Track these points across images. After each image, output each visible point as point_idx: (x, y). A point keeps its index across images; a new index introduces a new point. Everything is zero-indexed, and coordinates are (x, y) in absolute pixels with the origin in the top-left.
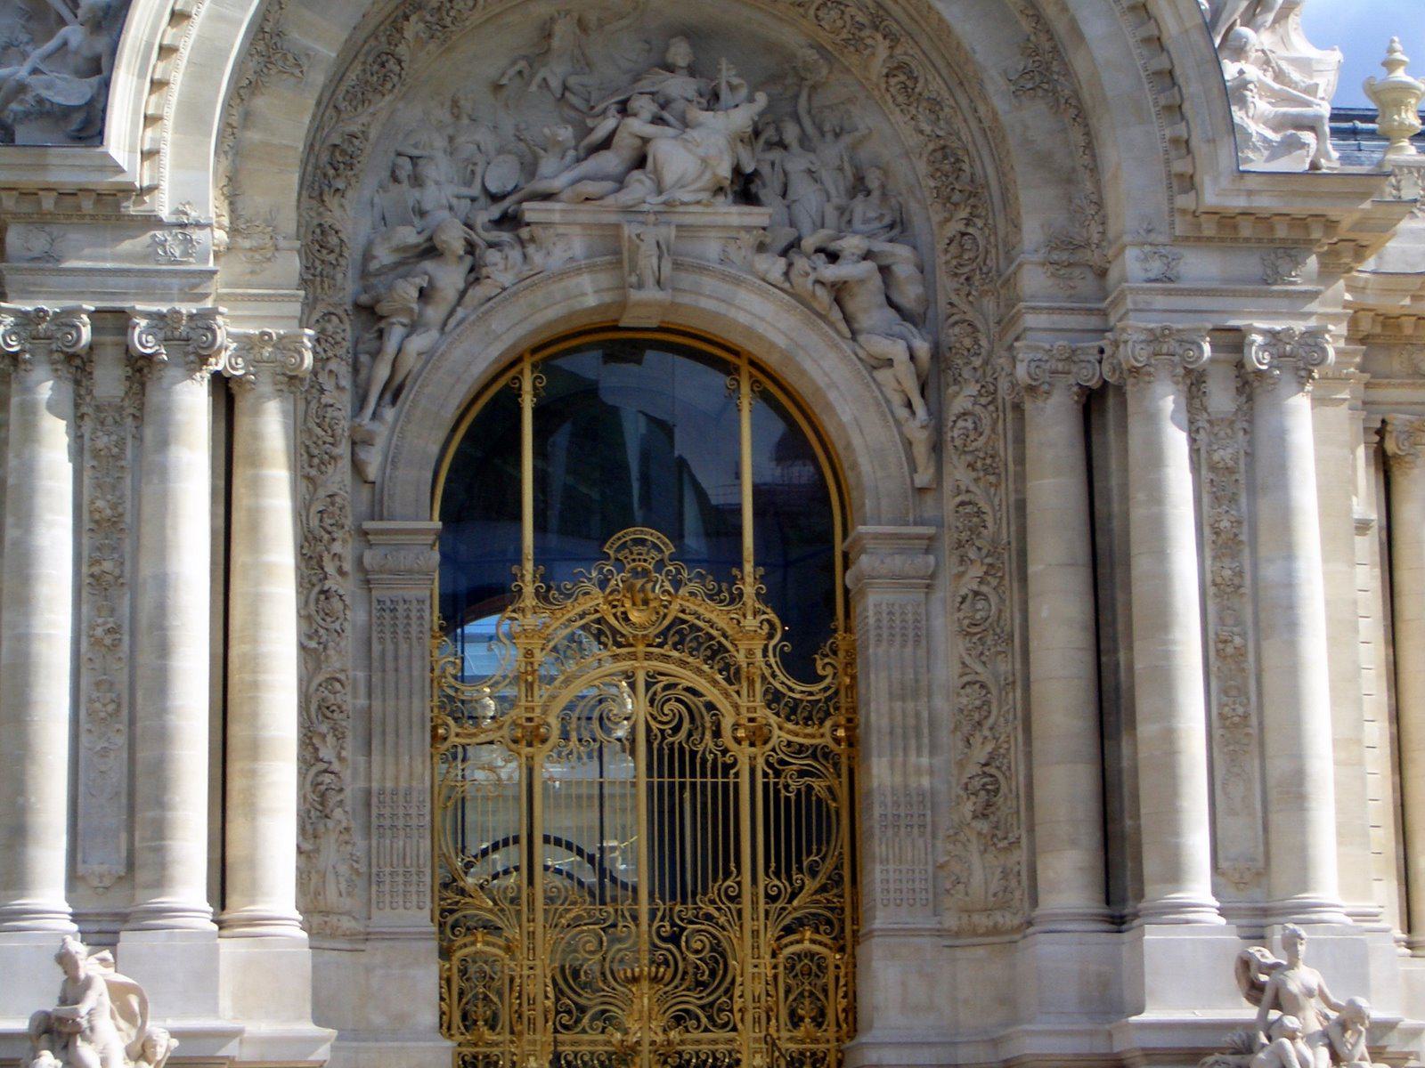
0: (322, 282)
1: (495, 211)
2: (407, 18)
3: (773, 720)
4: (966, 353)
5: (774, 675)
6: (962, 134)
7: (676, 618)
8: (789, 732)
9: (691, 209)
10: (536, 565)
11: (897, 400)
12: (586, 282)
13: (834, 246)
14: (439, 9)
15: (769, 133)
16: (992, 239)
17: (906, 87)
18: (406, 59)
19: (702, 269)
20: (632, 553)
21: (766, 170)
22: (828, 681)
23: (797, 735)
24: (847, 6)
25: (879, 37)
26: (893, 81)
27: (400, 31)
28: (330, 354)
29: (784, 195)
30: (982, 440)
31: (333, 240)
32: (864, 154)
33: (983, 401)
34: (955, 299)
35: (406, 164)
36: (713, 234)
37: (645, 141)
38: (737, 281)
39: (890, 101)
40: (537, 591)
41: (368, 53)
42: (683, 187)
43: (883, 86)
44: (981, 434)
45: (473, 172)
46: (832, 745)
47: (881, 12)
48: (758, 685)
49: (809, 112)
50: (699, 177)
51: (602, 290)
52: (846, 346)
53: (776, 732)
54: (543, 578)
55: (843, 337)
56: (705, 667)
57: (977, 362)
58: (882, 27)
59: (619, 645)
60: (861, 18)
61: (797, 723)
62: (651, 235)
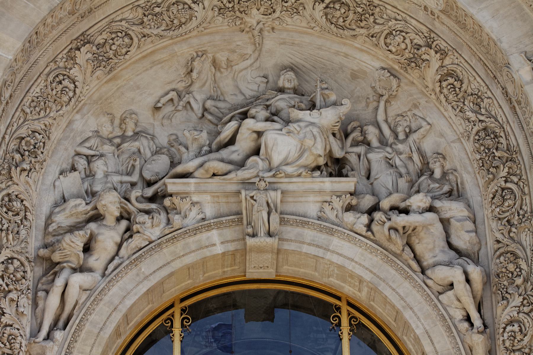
0: (7, 234)
1: (150, 192)
2: (78, 49)
4: (510, 275)
6: (499, 117)
9: (294, 180)
11: (459, 315)
12: (214, 235)
13: (403, 205)
14: (105, 43)
15: (356, 135)
16: (526, 190)
17: (454, 88)
18: (79, 78)
19: (304, 224)
21: (353, 158)
24: (407, 33)
25: (432, 52)
26: (444, 84)
27: (73, 58)
28: (11, 287)
29: (368, 178)
30: (526, 339)
31: (17, 205)
32: (428, 146)
33: (526, 309)
34: (500, 237)
35: (82, 163)
36: (312, 198)
37: (260, 134)
38: (331, 232)
39: (443, 100)
41: (48, 75)
42: (287, 164)
43: (438, 89)
44: (525, 335)
45: (133, 166)
47: (433, 35)
49: (386, 121)
50: (300, 156)
51: (228, 242)
52: (418, 278)
55: (414, 271)
57: (519, 281)
58: (433, 46)
60: (419, 41)
62: (261, 197)
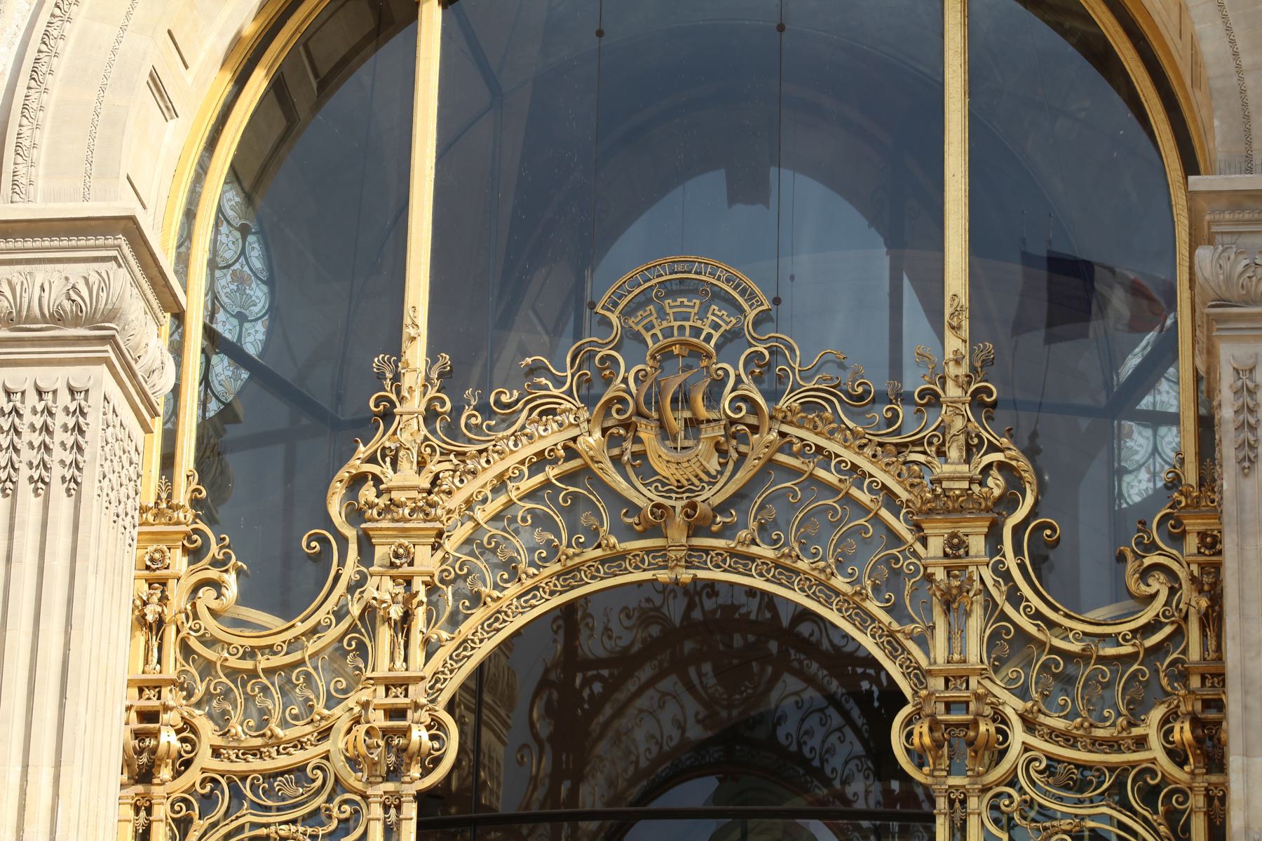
3: (1012, 706)
5: (1015, 597)
7: (771, 463)
8: (1053, 735)
10: (432, 354)
20: (662, 314)
22: (1157, 606)
23: (1069, 740)
40: (430, 416)
46: (1165, 763)
48: (975, 623)
53: (1018, 736)
54: (449, 381)
56: (839, 582)
59: (629, 533)
61: (1074, 715)
